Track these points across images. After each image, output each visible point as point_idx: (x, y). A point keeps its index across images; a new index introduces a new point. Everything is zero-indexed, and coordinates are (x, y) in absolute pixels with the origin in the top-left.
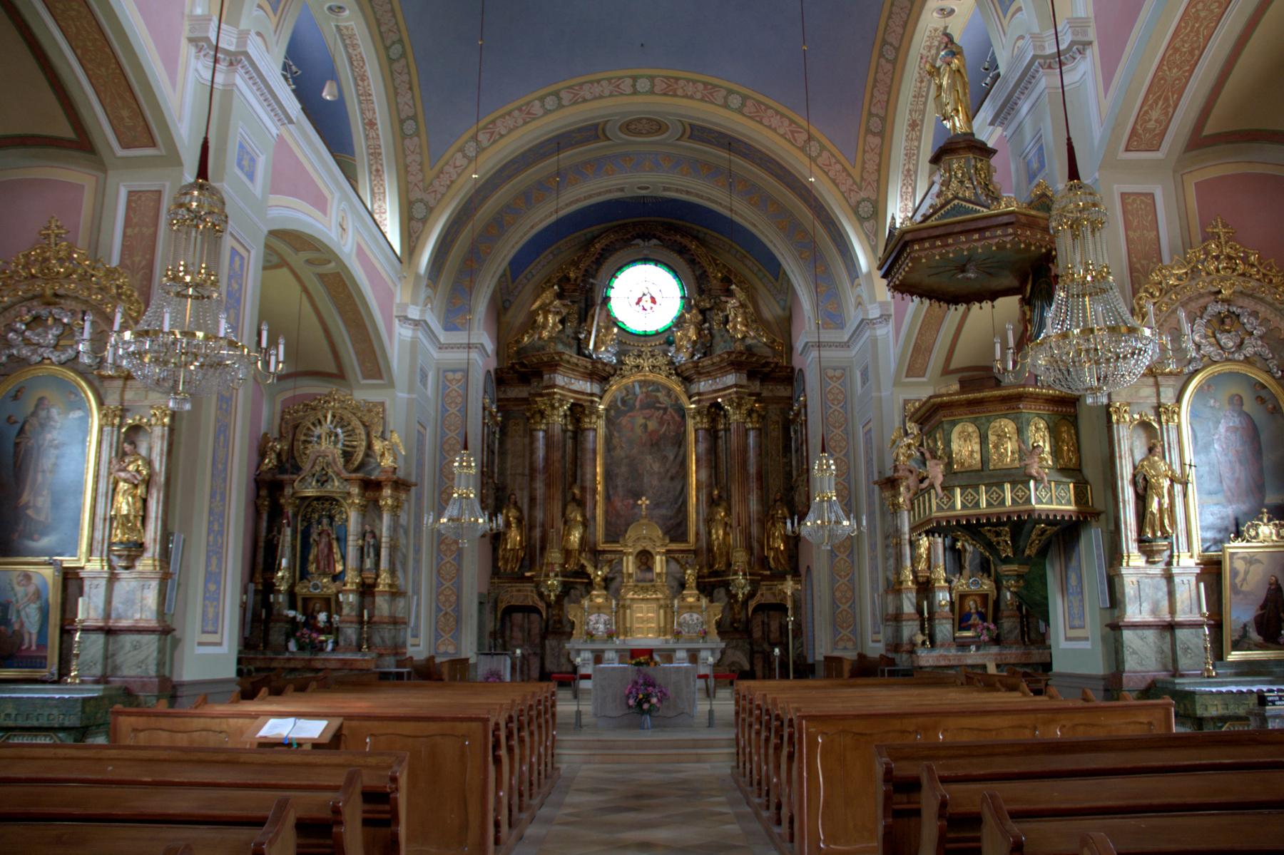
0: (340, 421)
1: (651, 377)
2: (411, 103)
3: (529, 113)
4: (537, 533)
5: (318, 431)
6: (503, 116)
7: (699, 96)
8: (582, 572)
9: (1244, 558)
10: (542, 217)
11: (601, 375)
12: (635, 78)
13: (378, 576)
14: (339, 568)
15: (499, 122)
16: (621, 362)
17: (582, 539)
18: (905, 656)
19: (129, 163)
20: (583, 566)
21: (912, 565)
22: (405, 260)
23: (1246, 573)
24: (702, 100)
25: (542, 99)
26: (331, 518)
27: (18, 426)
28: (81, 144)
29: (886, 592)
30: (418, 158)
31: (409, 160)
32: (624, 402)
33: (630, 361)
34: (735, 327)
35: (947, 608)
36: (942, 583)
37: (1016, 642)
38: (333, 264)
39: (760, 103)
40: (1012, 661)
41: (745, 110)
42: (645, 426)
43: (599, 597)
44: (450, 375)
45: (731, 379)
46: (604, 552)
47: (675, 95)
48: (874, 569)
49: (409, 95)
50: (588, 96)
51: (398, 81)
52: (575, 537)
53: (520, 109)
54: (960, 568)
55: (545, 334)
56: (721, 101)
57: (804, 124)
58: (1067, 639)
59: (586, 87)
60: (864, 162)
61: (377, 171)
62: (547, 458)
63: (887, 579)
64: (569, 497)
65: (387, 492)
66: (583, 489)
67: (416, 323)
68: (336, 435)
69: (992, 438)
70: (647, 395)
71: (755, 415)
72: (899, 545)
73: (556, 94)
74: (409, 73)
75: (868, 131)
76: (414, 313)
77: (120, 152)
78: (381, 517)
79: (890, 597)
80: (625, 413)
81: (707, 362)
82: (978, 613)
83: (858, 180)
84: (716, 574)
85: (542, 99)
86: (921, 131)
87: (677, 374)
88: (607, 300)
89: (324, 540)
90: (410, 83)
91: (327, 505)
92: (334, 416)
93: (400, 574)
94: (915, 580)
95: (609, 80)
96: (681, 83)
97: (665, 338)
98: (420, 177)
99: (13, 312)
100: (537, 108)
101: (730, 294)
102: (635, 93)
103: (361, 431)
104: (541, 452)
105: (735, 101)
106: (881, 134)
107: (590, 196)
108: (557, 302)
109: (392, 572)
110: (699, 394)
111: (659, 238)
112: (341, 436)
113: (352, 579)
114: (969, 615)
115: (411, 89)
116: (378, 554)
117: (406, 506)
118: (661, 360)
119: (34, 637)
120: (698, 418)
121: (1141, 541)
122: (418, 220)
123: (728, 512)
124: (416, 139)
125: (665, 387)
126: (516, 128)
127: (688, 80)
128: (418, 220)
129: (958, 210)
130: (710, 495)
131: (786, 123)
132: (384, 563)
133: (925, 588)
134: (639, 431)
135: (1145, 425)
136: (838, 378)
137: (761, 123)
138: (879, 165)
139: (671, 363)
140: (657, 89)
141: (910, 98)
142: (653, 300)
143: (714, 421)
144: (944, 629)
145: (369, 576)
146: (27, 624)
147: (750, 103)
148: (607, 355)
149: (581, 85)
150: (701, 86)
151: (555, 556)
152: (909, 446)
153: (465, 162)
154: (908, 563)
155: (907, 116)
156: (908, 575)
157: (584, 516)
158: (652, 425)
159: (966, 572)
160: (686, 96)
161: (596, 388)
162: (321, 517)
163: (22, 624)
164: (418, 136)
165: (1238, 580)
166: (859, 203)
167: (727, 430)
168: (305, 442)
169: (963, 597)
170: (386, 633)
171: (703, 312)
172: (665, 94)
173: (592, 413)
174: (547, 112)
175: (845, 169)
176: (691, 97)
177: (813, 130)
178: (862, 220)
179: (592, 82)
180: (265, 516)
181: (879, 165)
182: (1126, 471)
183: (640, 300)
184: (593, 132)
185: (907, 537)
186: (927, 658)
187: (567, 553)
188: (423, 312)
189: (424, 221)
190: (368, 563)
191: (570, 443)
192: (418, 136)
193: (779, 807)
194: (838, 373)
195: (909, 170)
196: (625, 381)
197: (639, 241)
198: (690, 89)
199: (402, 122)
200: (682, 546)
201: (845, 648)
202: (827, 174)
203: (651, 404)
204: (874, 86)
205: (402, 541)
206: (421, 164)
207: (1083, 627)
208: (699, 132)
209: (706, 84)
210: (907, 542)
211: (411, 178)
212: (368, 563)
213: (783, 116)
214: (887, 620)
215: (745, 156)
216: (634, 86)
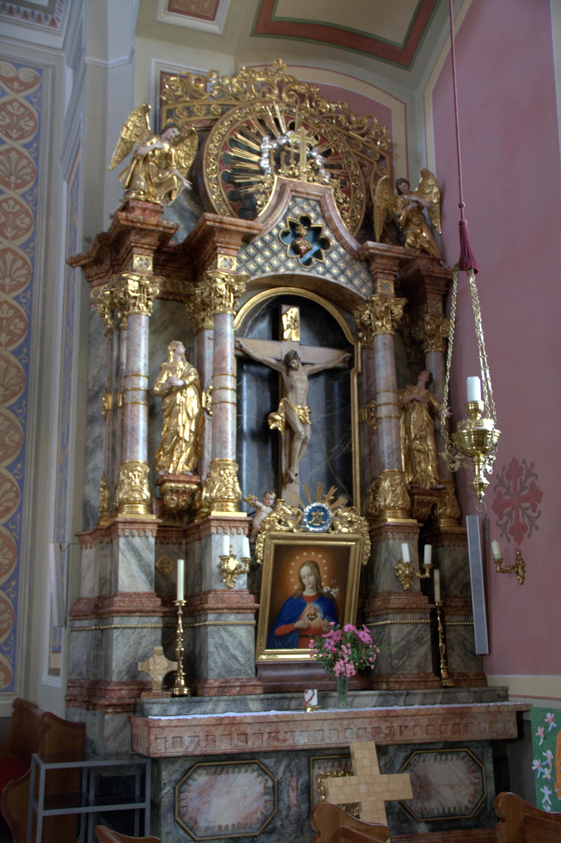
18: (112, 722)
21: (152, 461)
29: (80, 539)
35: (242, 581)
37: (423, 681)
40: (419, 735)
54: (279, 482)
63: (86, 506)
72: (119, 412)
82: (321, 598)
94: (158, 502)
133: (183, 524)
136: (26, 86)
144: (231, 641)
154: (141, 454)
156: (137, 485)
159: (292, 491)
169: (283, 552)
185: (143, 383)
194: (25, 75)
210: (140, 396)
214: (76, 615)
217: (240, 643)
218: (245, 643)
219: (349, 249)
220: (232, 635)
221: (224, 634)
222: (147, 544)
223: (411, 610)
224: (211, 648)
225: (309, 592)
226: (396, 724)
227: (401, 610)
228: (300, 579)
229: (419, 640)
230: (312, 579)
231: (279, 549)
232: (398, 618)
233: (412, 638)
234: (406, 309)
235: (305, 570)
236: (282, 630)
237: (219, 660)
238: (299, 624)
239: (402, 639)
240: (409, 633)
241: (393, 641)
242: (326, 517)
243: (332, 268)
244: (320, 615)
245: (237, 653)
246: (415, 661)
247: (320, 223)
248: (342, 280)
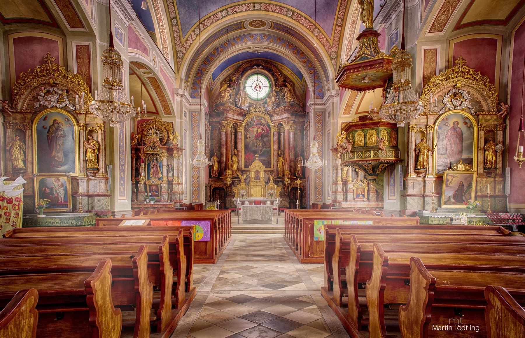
0: (158, 129)
1: (259, 115)
2: (174, 12)
3: (217, 17)
4: (223, 165)
5: (151, 132)
6: (208, 18)
7: (277, 11)
8: (237, 177)
9: (451, 176)
10: (222, 59)
12: (254, 4)
13: (173, 178)
14: (160, 176)
15: (206, 21)
16: (250, 110)
17: (238, 167)
18: (338, 204)
19: (74, 34)
20: (238, 175)
22: (176, 72)
23: (452, 180)
24: (278, 13)
25: (221, 12)
26: (157, 160)
27: (47, 129)
28: (53, 25)
29: (333, 184)
30: (178, 34)
31: (175, 35)
33: (253, 109)
34: (287, 97)
36: (351, 182)
38: (152, 74)
39: (298, 14)
41: (293, 17)
42: (258, 131)
43: (243, 184)
44: (194, 113)
45: (285, 115)
46: (245, 171)
47: (269, 11)
48: (329, 177)
49: (173, 8)
50: (238, 11)
52: (236, 165)
55: (225, 99)
56: (285, 13)
57: (314, 22)
58: (389, 199)
59: (237, 7)
60: (334, 37)
61: (164, 38)
62: (226, 141)
63: (333, 180)
64: (233, 154)
65: (175, 152)
66: (238, 151)
67: (182, 96)
68: (157, 133)
69: (368, 136)
71: (293, 127)
72: (337, 169)
73: (226, 9)
75: (337, 25)
76: (181, 92)
77: (70, 29)
78: (173, 160)
79: (334, 186)
80: (250, 126)
81: (277, 110)
83: (331, 44)
84: (279, 178)
85: (221, 12)
86: (356, 24)
87: (268, 114)
88: (245, 87)
89: (155, 167)
91: (155, 156)
92: (156, 127)
93: (180, 177)
94: (342, 181)
95: (245, 4)
96: (271, 5)
97: (263, 102)
98: (179, 42)
99: (38, 89)
100: (219, 16)
101: (286, 86)
102: (254, 10)
103: (165, 132)
104: (224, 139)
105: (290, 13)
106: (341, 26)
107: (239, 50)
108: (228, 89)
109: (178, 177)
110: (275, 120)
111: (262, 66)
112: (159, 133)
113: (165, 179)
116: (173, 172)
117: (181, 156)
118: (263, 109)
119: (63, 199)
120: (274, 128)
121: (416, 169)
122: (180, 58)
123: (284, 158)
125: (264, 118)
126: (212, 23)
127: (273, 5)
128: (180, 58)
129: (364, 58)
130: (278, 153)
131: (308, 22)
132: (175, 174)
134: (255, 133)
135: (422, 132)
137: (299, 22)
138: (339, 38)
139: (266, 110)
140: (262, 8)
141: (354, 11)
142: (260, 87)
143: (279, 129)
145: (170, 179)
146: (59, 194)
147: (295, 14)
148: (245, 107)
149: (235, 6)
150: (278, 7)
151: (229, 172)
152: (342, 138)
153: (195, 36)
154: (340, 175)
155: (352, 18)
156: (339, 179)
157: (238, 159)
158: (260, 130)
160: (272, 11)
161: (241, 118)
162: (153, 160)
163: (58, 195)
164: (178, 25)
165: (448, 183)
166: (331, 53)
167: (284, 132)
168: (146, 135)
170: (177, 196)
171: (276, 92)
172: (265, 10)
173: (240, 127)
175: (327, 40)
176: (274, 12)
177: (317, 25)
178: (332, 59)
179: (239, 5)
180: (134, 160)
181: (339, 38)
182: (412, 147)
183: (256, 87)
184: (240, 25)
186: (345, 205)
187: (233, 171)
188: (184, 92)
189: (182, 58)
190: (170, 174)
191: (233, 136)
192: (178, 25)
193: (297, 245)
195: (350, 40)
196: (251, 116)
197: (256, 67)
198: (274, 8)
199: (171, 19)
200: (270, 169)
201: (319, 201)
202: (321, 42)
204: (340, 6)
205: (181, 167)
207: (394, 196)
208: (277, 26)
209: (279, 6)
211: (176, 42)
212: (170, 174)
213: (307, 19)
215: (292, 35)
216: (254, 7)
222: (341, 185)
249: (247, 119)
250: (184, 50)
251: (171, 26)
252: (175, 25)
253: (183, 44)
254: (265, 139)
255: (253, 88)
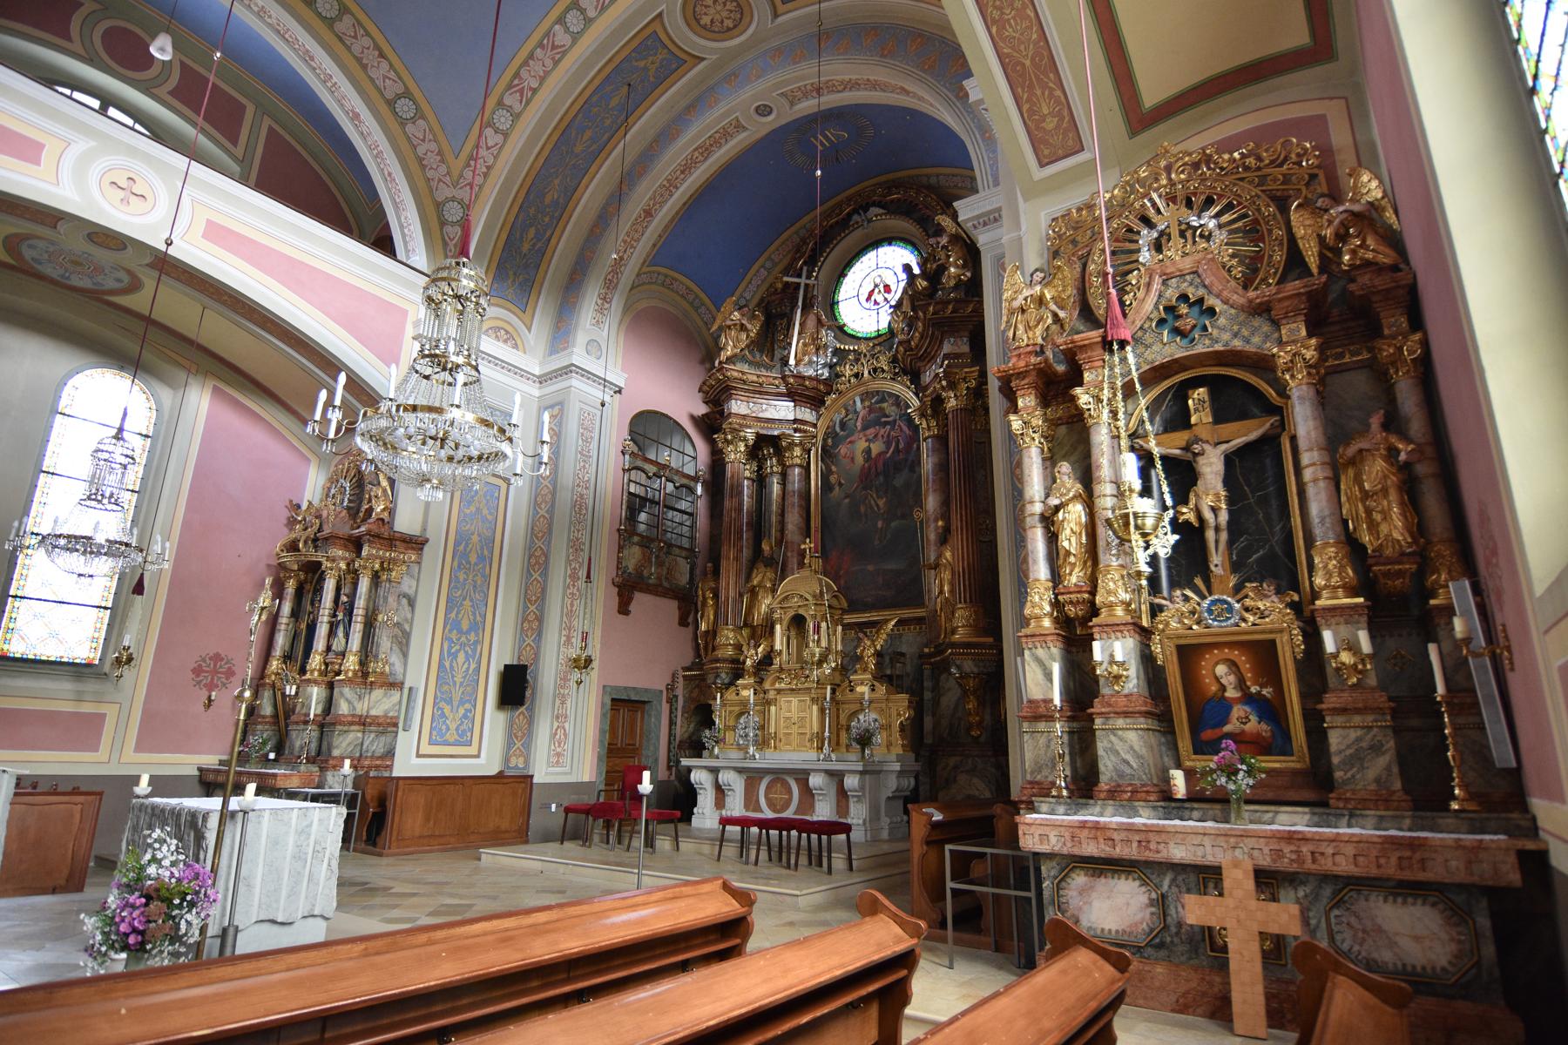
2: (392, 75)
3: (554, 47)
6: (525, 63)
11: (808, 394)
15: (524, 73)
30: (433, 146)
31: (421, 150)
32: (843, 425)
37: (1380, 800)
42: (868, 451)
51: (356, 49)
53: (540, 45)
70: (870, 412)
74: (367, 34)
82: (1248, 698)
85: (561, 20)
90: (377, 47)
98: (443, 169)
100: (562, 38)
111: (880, 205)
114: (1222, 707)
115: (382, 55)
122: (453, 224)
124: (421, 122)
126: (547, 74)
134: (860, 460)
144: (1124, 745)
153: (499, 138)
158: (876, 448)
164: (423, 117)
169: (1189, 653)
174: (576, 37)
183: (871, 293)
192: (423, 117)
197: (856, 217)
199: (391, 103)
203: (876, 419)
206: (440, 153)
217: (1132, 748)
218: (1137, 748)
219: (1242, 309)
220: (1121, 739)
221: (1113, 738)
223: (1358, 711)
224: (1101, 752)
225: (1231, 693)
226: (1306, 849)
227: (1343, 711)
228: (1217, 679)
229: (1376, 749)
230: (1232, 678)
231: (1180, 648)
232: (1339, 720)
233: (1364, 745)
234: (1321, 349)
235: (1221, 670)
236: (1208, 734)
237: (1109, 764)
238: (1227, 728)
239: (1348, 747)
240: (1359, 740)
241: (1333, 748)
242: (1230, 609)
243: (1224, 334)
244: (1254, 718)
245: (1128, 757)
246: (1371, 774)
247: (1201, 292)
248: (1237, 344)
249: (833, 412)
250: (464, 194)
251: (394, 126)
252: (413, 120)
253: (461, 176)
254: (898, 482)
255: (863, 298)
